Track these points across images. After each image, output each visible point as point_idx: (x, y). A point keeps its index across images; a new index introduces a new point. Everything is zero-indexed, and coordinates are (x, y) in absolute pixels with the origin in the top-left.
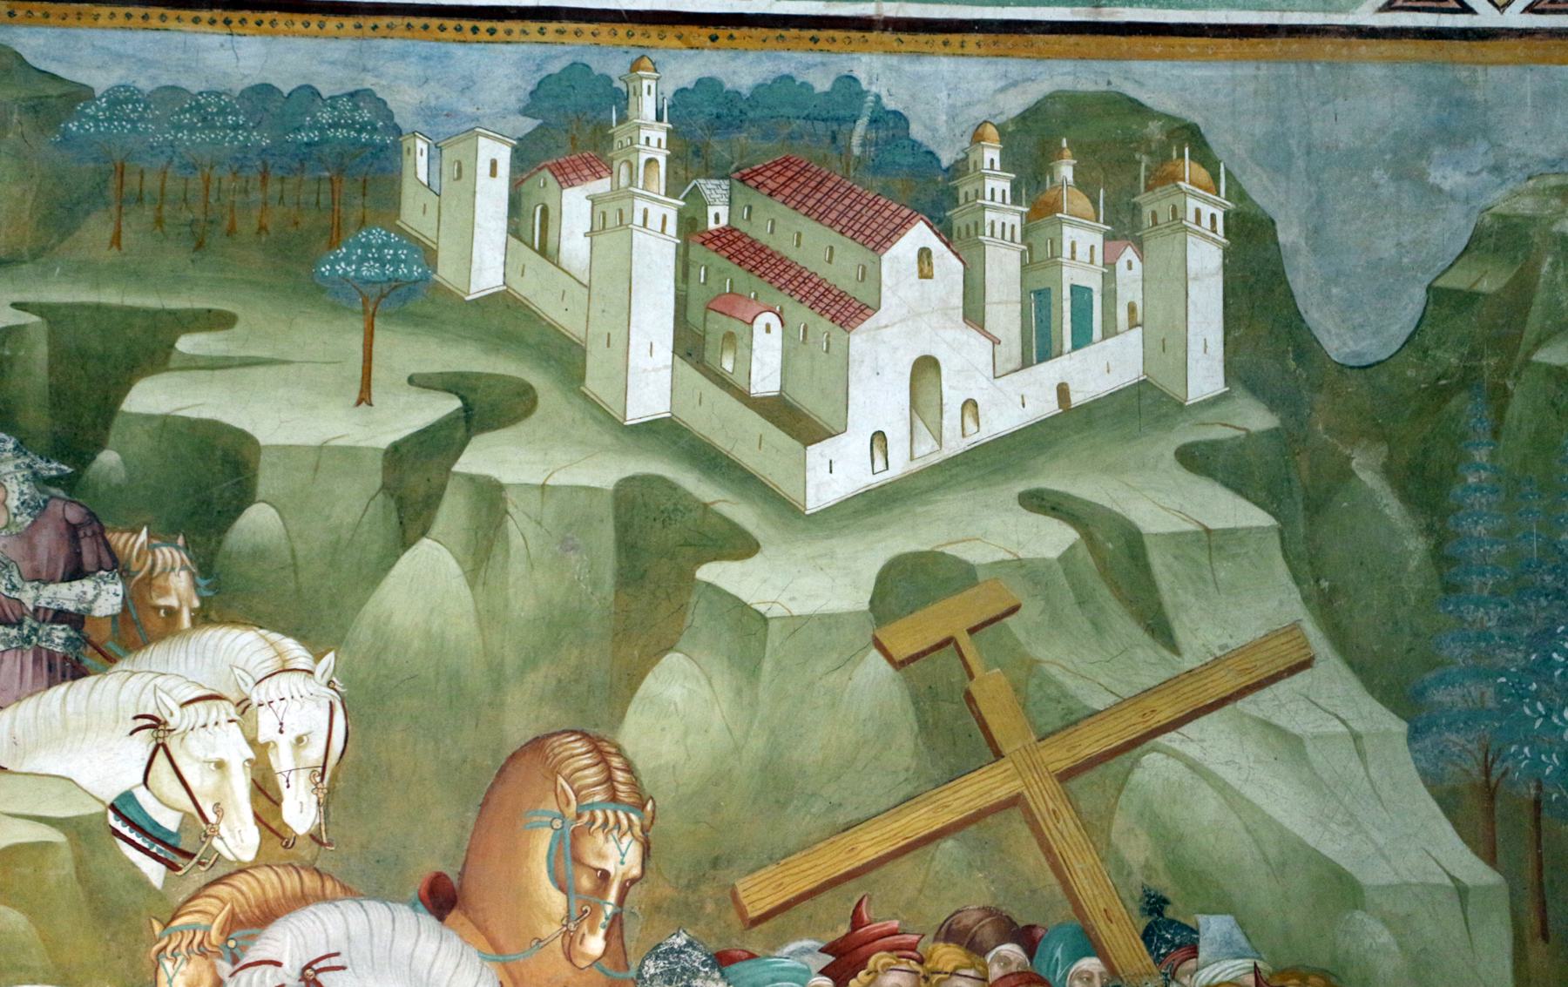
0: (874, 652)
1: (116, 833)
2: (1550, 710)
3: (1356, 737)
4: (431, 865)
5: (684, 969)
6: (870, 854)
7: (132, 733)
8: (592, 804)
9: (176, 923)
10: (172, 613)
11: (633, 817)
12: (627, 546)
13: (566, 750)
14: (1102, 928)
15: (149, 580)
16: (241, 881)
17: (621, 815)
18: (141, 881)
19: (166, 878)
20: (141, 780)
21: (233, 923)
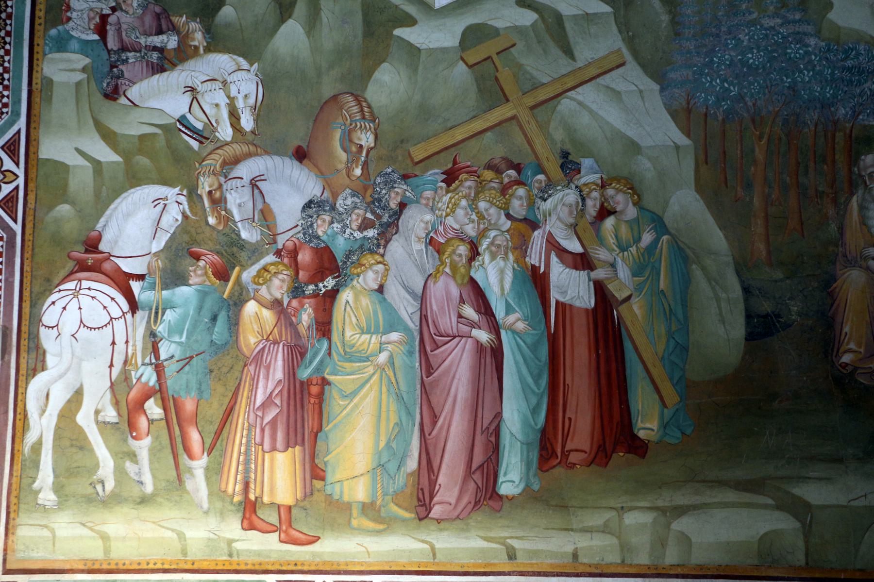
0: (461, 62)
1: (180, 130)
2: (712, 80)
3: (641, 92)
4: (296, 143)
5: (391, 180)
10: (196, 48)
11: (371, 125)
12: (367, 23)
14: (546, 164)
16: (226, 148)
17: (367, 124)
18: (190, 148)
21: (225, 163)
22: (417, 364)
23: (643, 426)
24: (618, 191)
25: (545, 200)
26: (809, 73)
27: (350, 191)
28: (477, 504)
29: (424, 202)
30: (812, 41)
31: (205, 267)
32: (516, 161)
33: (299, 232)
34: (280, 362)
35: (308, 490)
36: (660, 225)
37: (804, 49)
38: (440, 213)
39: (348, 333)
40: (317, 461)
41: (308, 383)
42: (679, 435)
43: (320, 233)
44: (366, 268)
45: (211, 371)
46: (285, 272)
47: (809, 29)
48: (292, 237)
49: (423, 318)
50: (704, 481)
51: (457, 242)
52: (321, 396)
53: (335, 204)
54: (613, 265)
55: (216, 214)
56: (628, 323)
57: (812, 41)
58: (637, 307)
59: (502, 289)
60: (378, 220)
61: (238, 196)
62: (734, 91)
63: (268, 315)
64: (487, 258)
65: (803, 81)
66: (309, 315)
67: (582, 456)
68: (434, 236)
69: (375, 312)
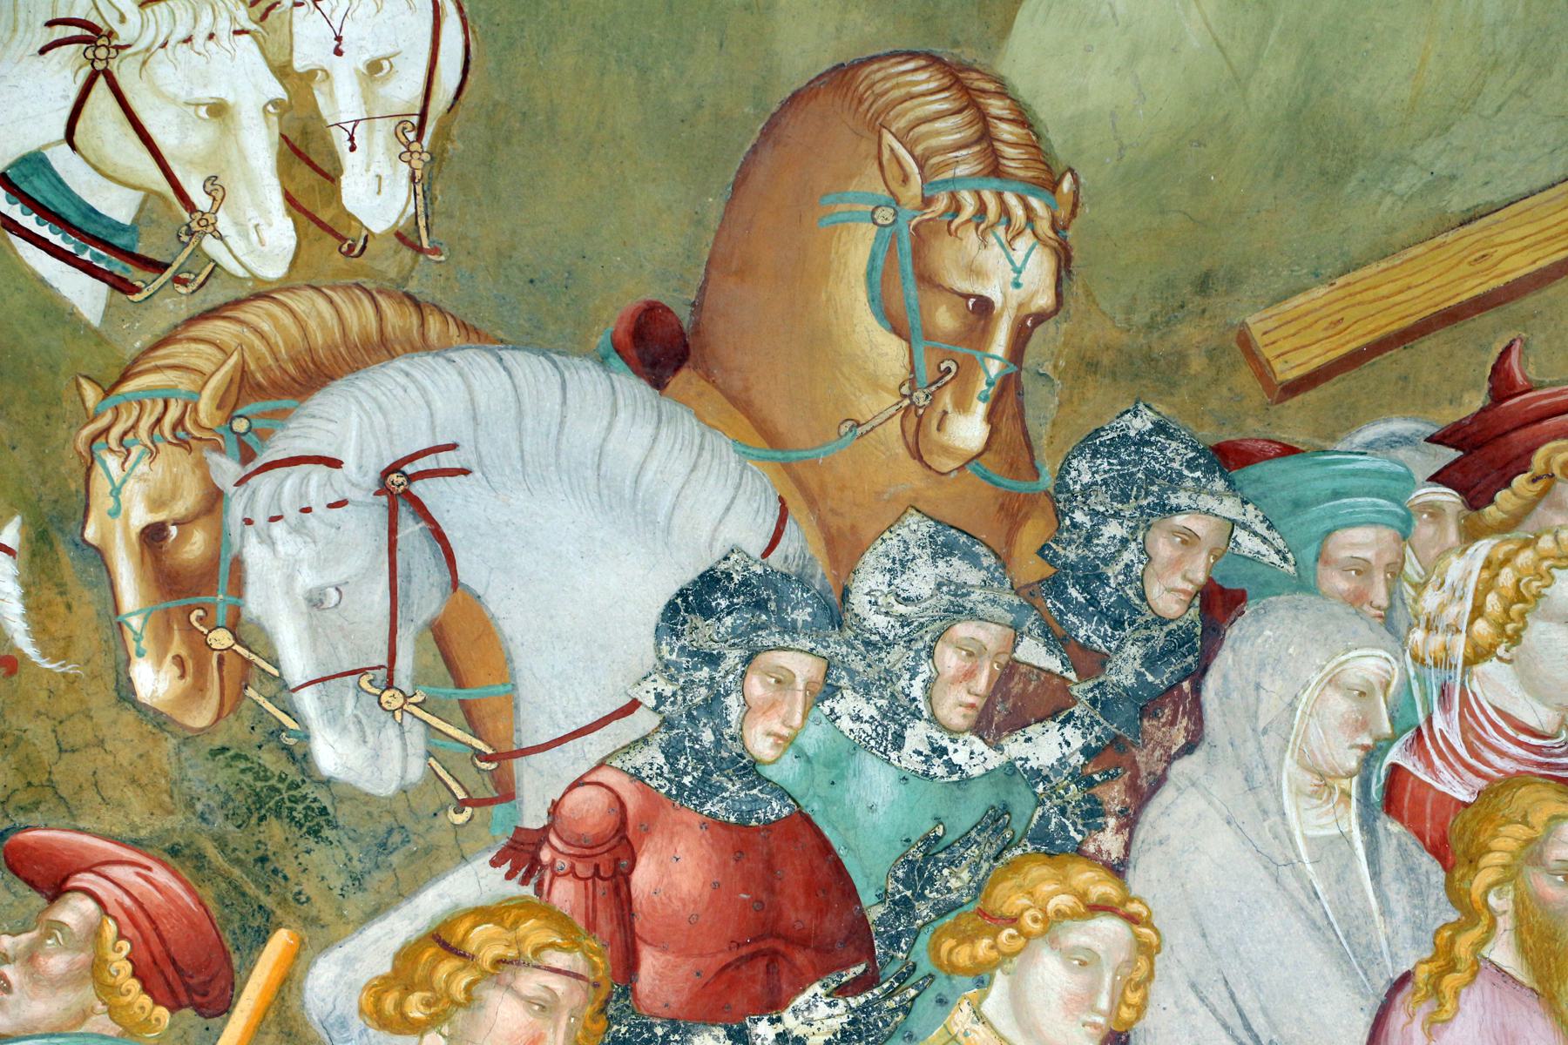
5: (1151, 475)
6: (1520, 266)
7: (43, 51)
8: (954, 180)
9: (130, 386)
11: (1035, 202)
13: (897, 86)
16: (256, 314)
19: (108, 306)
20: (60, 132)
21: (243, 387)
27: (926, 527)
29: (1341, 584)
31: (96, 933)
33: (645, 740)
38: (1436, 641)
43: (760, 745)
44: (1028, 936)
46: (559, 960)
48: (601, 764)
53: (845, 593)
55: (177, 646)
60: (1083, 676)
61: (306, 553)
68: (1408, 764)
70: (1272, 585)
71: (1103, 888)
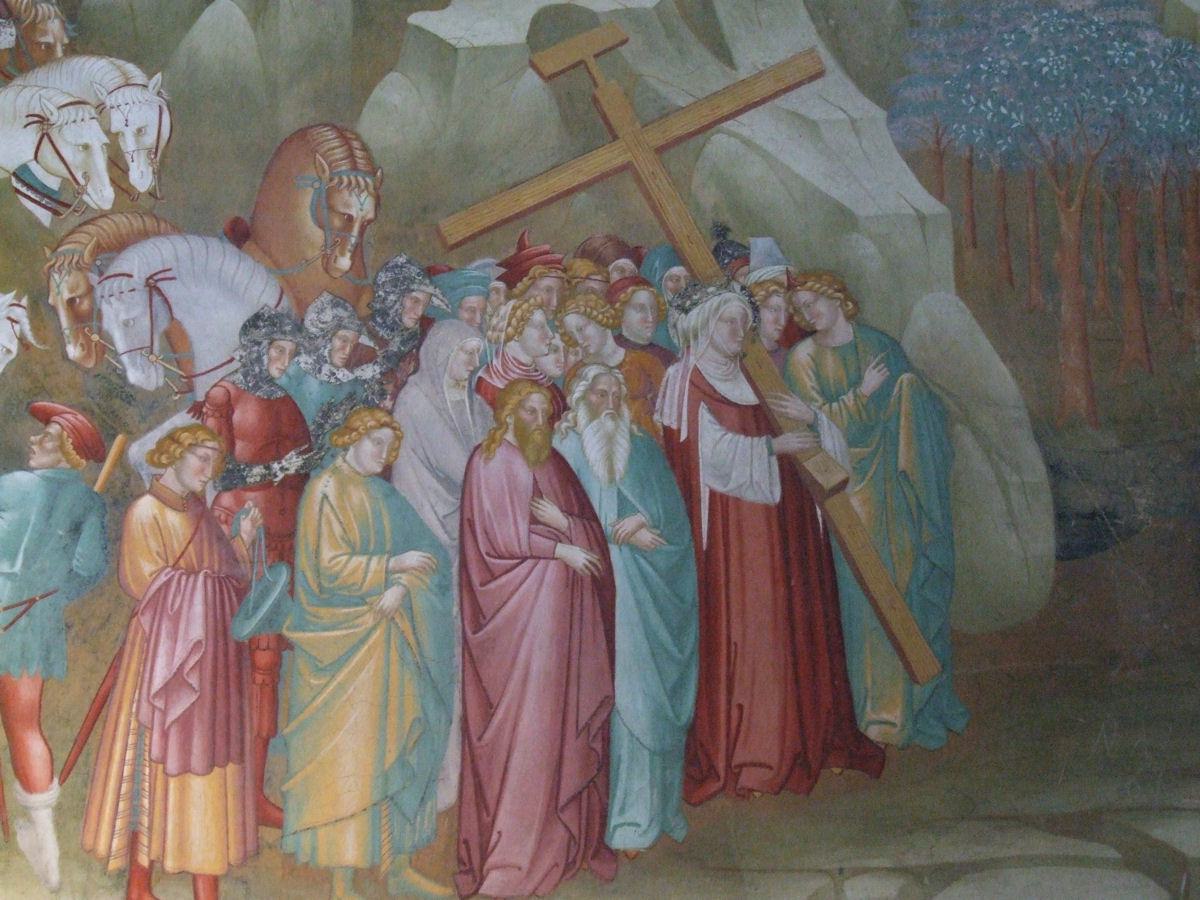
0: (530, 70)
1: (18, 191)
2: (978, 102)
3: (853, 122)
4: (233, 212)
5: (405, 278)
6: (530, 202)
7: (25, 126)
8: (339, 172)
9: (60, 250)
10: (50, 47)
11: (368, 180)
13: (322, 137)
14: (687, 249)
15: (33, 24)
16: (101, 222)
17: (360, 179)
18: (38, 224)
19: (52, 220)
20: (32, 157)
21: (99, 249)
22: (456, 609)
23: (874, 717)
24: (818, 294)
25: (686, 311)
26: (1146, 90)
27: (330, 297)
28: (569, 868)
29: (466, 315)
30: (1149, 37)
31: (60, 436)
32: (633, 242)
33: (236, 371)
34: (198, 608)
35: (250, 847)
36: (895, 355)
37: (1137, 49)
38: (495, 334)
39: (327, 554)
40: (267, 791)
41: (253, 644)
42: (941, 732)
43: (274, 372)
44: (360, 434)
45: (69, 627)
46: (210, 444)
47: (1144, 16)
48: (222, 379)
49: (467, 525)
50: (990, 818)
51: (526, 388)
52: (274, 670)
53: (303, 320)
54: (812, 427)
55: (81, 340)
56: (844, 531)
57: (1149, 37)
58: (857, 500)
59: (611, 471)
60: (381, 348)
61: (122, 307)
62: (1018, 120)
63: (175, 520)
64: (582, 414)
65: (1137, 103)
66: (254, 521)
67: (766, 775)
68: (485, 376)
69: (377, 516)
70: (445, 316)
71: (386, 419)
